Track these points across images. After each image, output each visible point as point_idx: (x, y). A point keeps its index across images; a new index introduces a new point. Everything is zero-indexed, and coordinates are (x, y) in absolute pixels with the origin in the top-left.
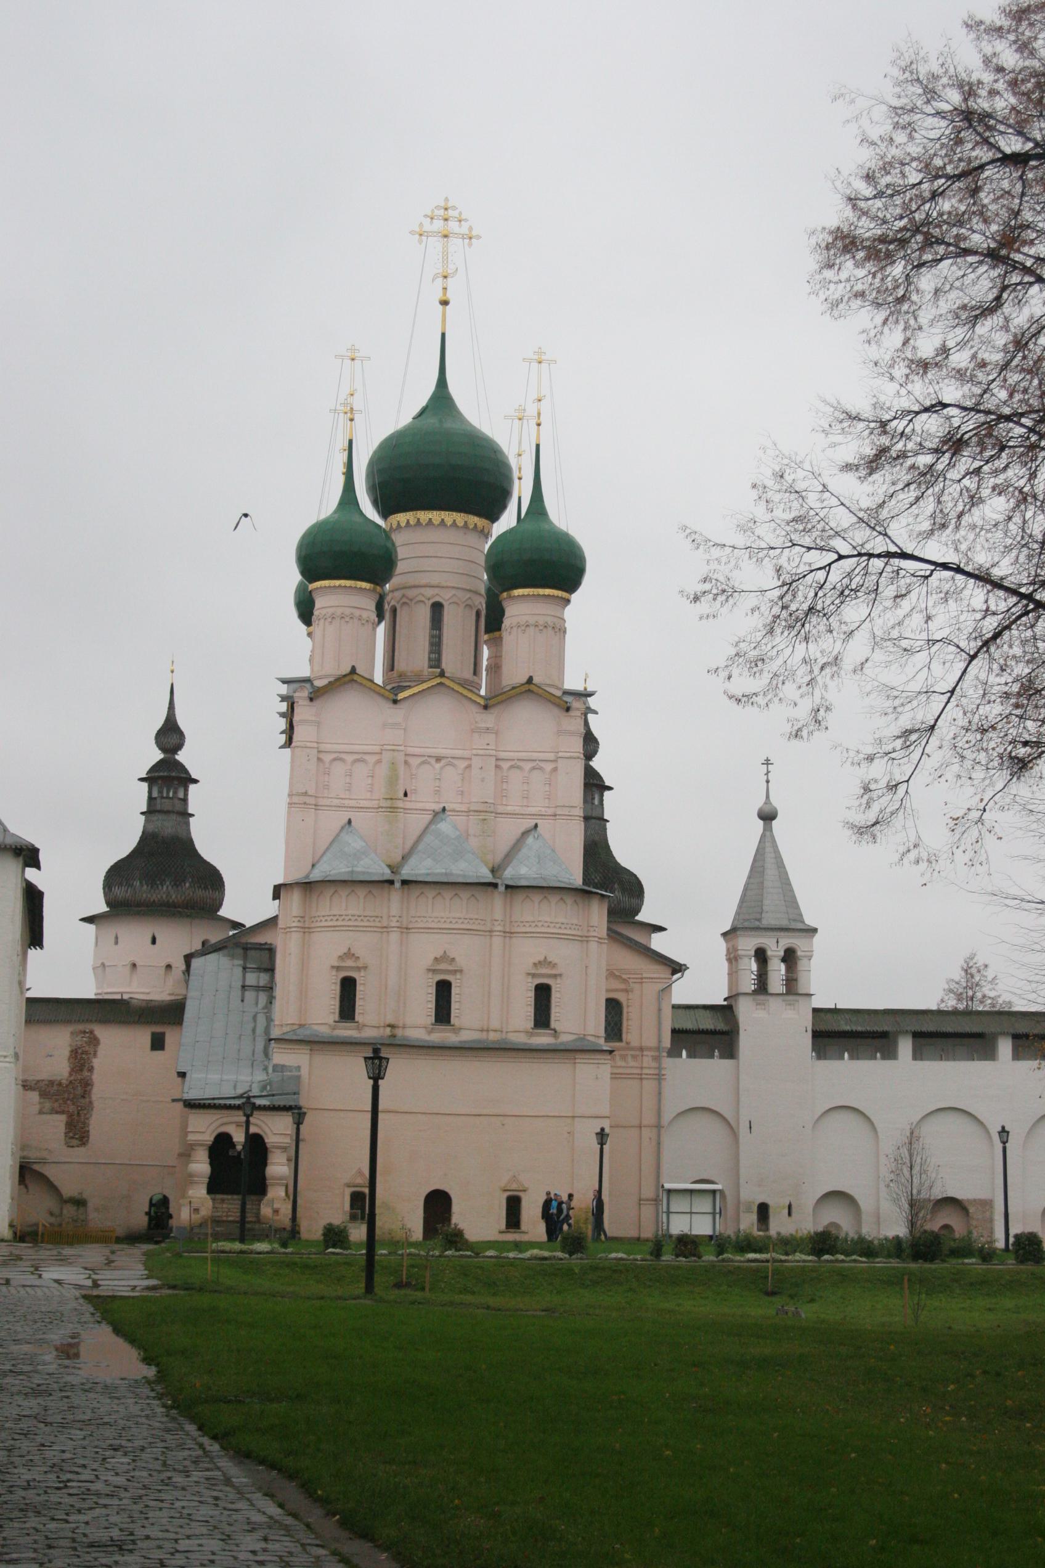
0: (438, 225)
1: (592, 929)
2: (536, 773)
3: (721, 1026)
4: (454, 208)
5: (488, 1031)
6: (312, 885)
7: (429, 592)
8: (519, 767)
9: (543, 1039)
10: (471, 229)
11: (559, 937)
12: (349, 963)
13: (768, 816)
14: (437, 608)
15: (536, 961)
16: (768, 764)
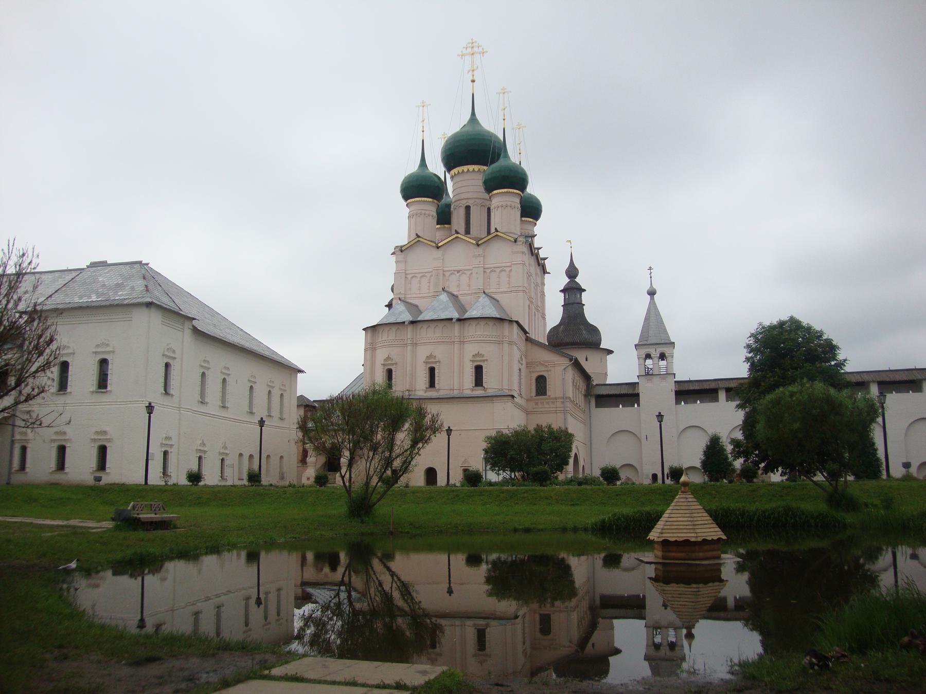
0: (469, 50)
1: (504, 337)
2: (502, 273)
3: (630, 392)
4: (476, 42)
5: (453, 390)
6: (376, 328)
7: (464, 202)
8: (495, 271)
9: (479, 392)
10: (483, 49)
11: (484, 342)
12: (390, 362)
13: (652, 293)
14: (468, 208)
15: (474, 354)
16: (650, 269)
